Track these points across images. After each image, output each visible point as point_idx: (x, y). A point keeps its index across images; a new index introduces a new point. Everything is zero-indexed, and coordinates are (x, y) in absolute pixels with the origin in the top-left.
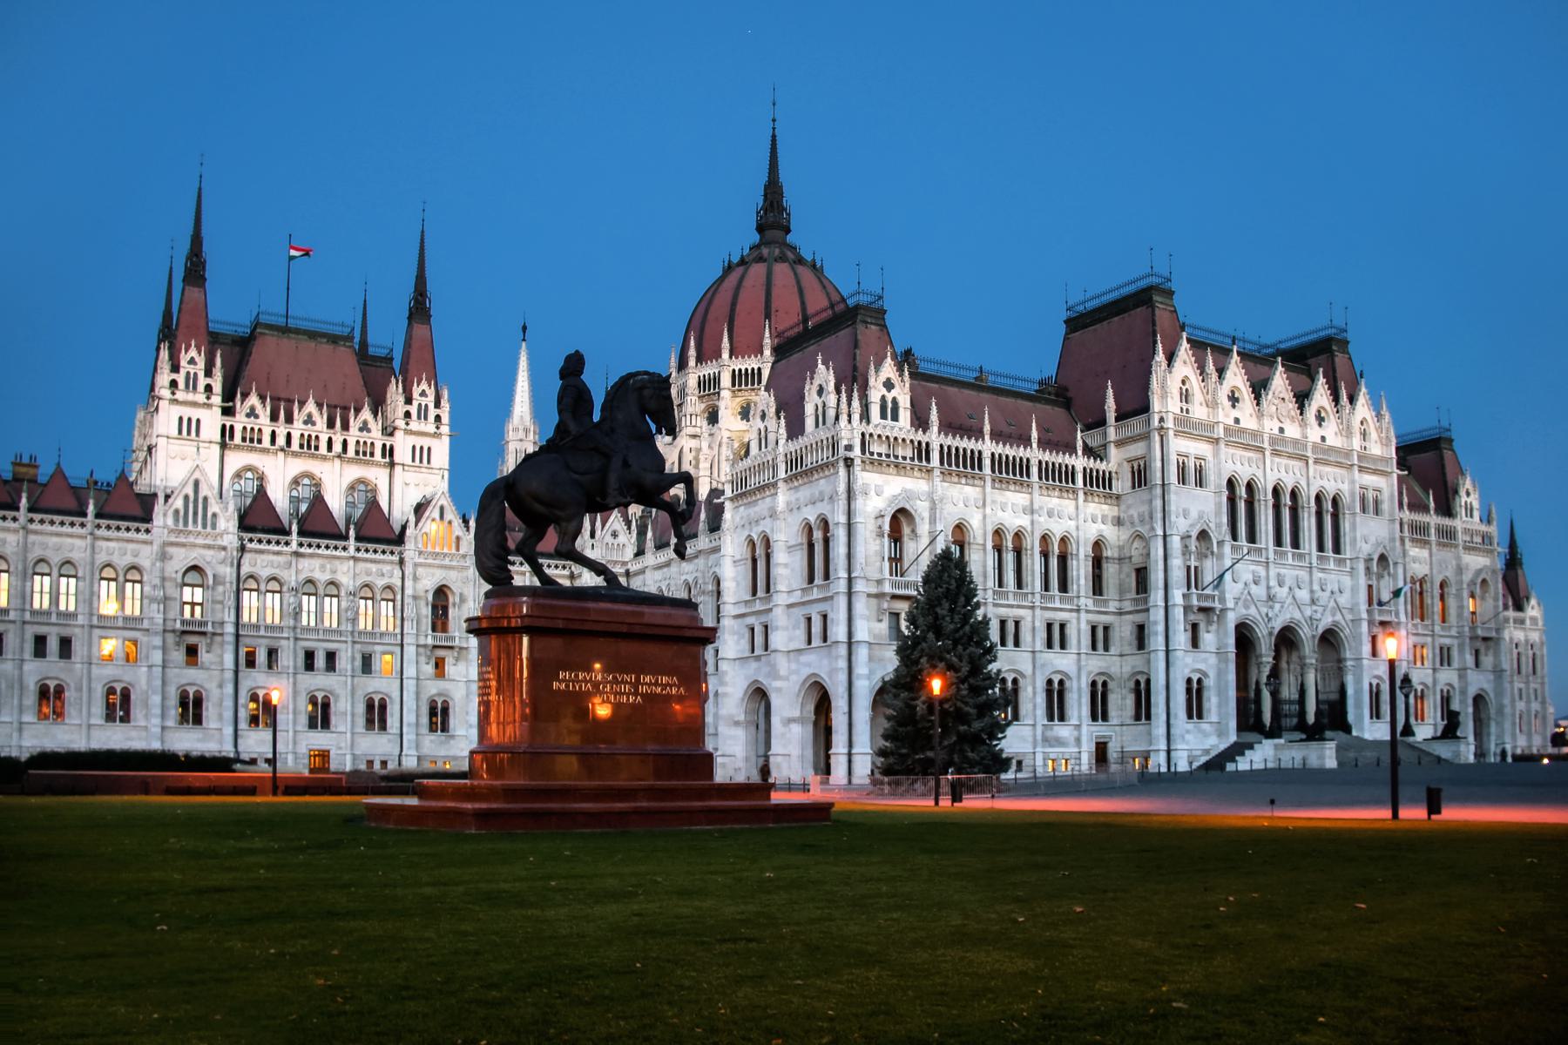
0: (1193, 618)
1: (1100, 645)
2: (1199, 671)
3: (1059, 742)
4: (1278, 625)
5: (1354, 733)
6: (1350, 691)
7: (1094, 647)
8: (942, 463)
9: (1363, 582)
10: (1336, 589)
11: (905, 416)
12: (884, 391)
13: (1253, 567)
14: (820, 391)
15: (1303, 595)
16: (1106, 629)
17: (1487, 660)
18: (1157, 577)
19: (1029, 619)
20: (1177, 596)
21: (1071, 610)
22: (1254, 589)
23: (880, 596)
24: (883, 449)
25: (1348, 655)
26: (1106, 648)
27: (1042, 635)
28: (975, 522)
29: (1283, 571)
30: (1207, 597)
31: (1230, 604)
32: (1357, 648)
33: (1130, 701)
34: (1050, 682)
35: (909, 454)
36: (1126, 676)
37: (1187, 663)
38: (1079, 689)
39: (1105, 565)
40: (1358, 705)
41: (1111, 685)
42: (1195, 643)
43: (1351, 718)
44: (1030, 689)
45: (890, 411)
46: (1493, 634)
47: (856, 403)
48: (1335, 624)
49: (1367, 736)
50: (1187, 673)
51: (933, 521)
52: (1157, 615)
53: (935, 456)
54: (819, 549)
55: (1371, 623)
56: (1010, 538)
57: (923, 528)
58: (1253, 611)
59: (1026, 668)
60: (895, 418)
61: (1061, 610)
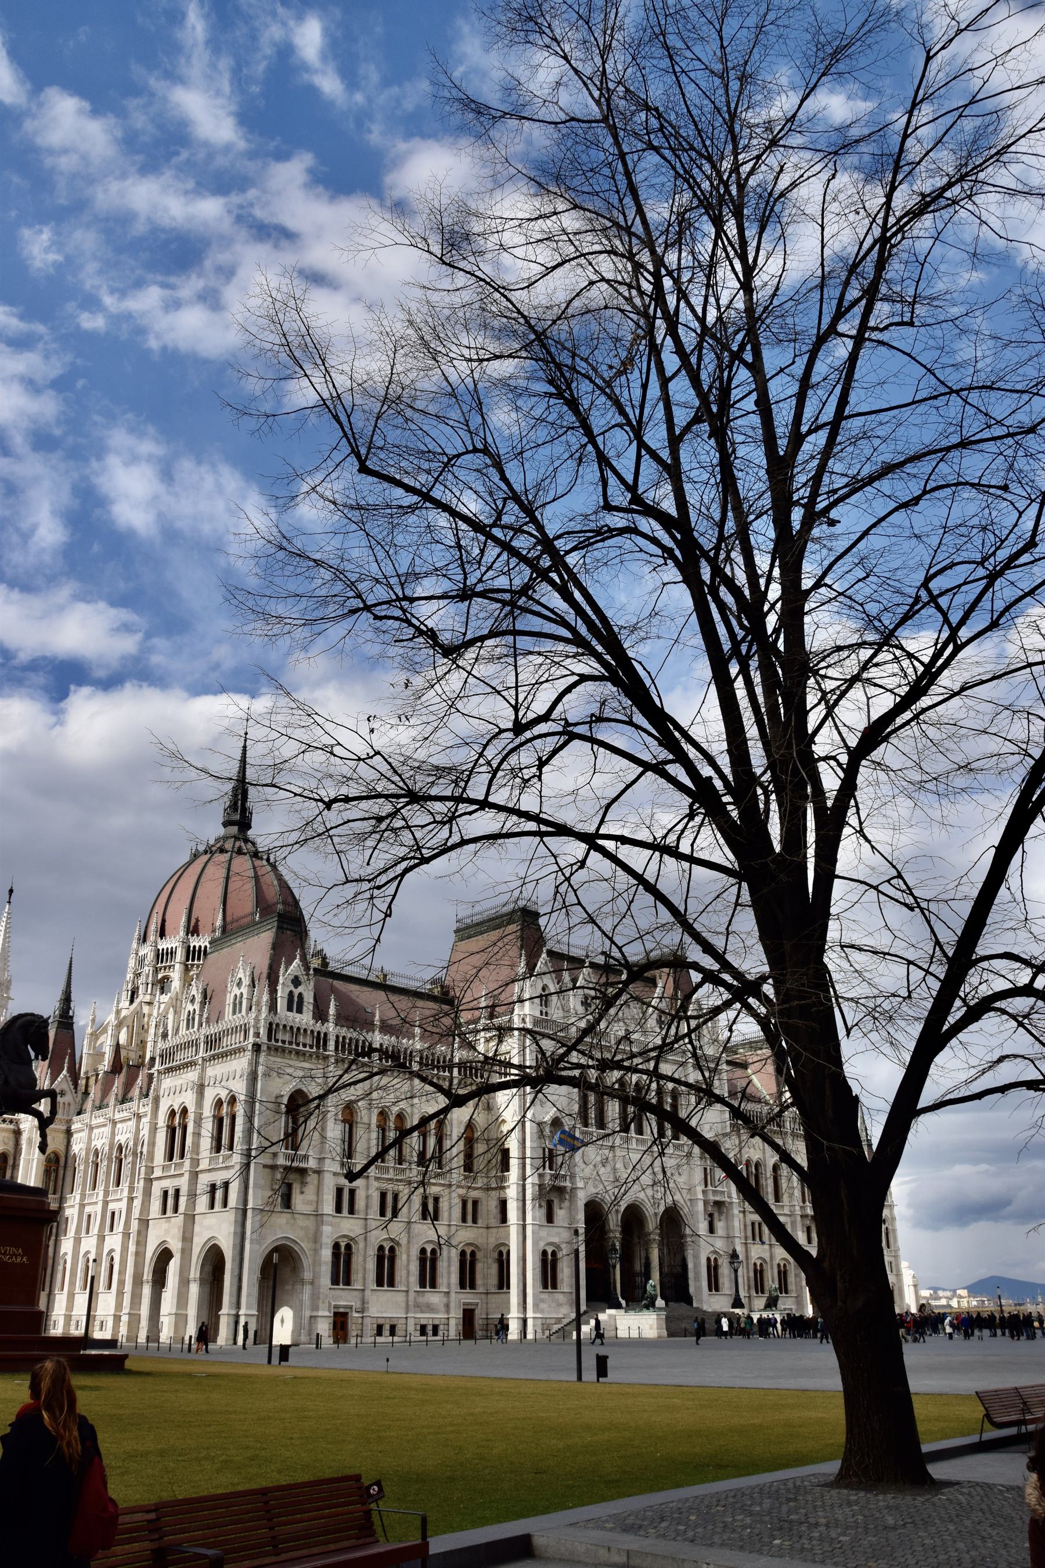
1: (470, 1217)
7: (464, 1219)
12: (292, 988)
14: (239, 984)
16: (475, 1203)
22: (602, 1171)
23: (273, 1167)
24: (287, 1037)
26: (475, 1221)
31: (580, 1184)
33: (494, 1269)
34: (423, 1251)
36: (491, 1246)
42: (550, 1218)
44: (404, 1257)
47: (265, 997)
50: (542, 1245)
54: (226, 1122)
55: (706, 1203)
56: (392, 1118)
60: (300, 1011)
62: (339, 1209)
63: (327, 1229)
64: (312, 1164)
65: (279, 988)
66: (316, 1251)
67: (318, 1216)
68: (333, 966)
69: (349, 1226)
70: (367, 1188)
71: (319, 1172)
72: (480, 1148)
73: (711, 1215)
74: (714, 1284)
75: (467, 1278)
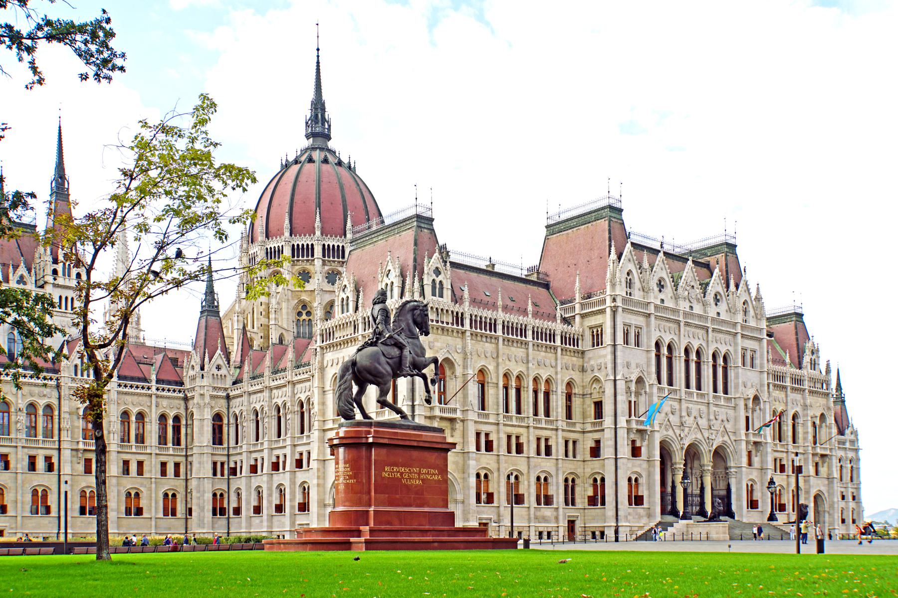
0: (632, 436)
2: (636, 473)
3: (545, 519)
4: (687, 443)
5: (736, 518)
6: (733, 489)
8: (471, 327)
9: (742, 414)
10: (725, 419)
11: (447, 293)
12: (434, 276)
13: (671, 403)
15: (703, 423)
16: (574, 442)
17: (823, 470)
18: (608, 408)
19: (525, 434)
20: (622, 422)
21: (552, 429)
22: (671, 417)
25: (731, 463)
27: (534, 446)
28: (491, 368)
29: (690, 406)
30: (642, 422)
31: (657, 428)
32: (738, 460)
35: (450, 321)
37: (629, 467)
38: (557, 483)
39: (573, 399)
40: (739, 499)
41: (577, 481)
43: (734, 508)
45: (438, 290)
46: (828, 452)
48: (724, 442)
49: (745, 520)
50: (628, 474)
51: (465, 367)
52: (608, 434)
53: (467, 322)
55: (747, 442)
56: (514, 379)
57: (459, 371)
58: (670, 432)
59: (523, 468)
60: (441, 296)
61: (546, 429)
62: (478, 449)
63: (472, 463)
64: (459, 415)
65: (425, 277)
66: (465, 480)
67: (465, 454)
68: (454, 258)
69: (487, 460)
70: (498, 432)
71: (463, 421)
72: (576, 402)
73: (750, 453)
74: (753, 504)
75: (570, 500)
